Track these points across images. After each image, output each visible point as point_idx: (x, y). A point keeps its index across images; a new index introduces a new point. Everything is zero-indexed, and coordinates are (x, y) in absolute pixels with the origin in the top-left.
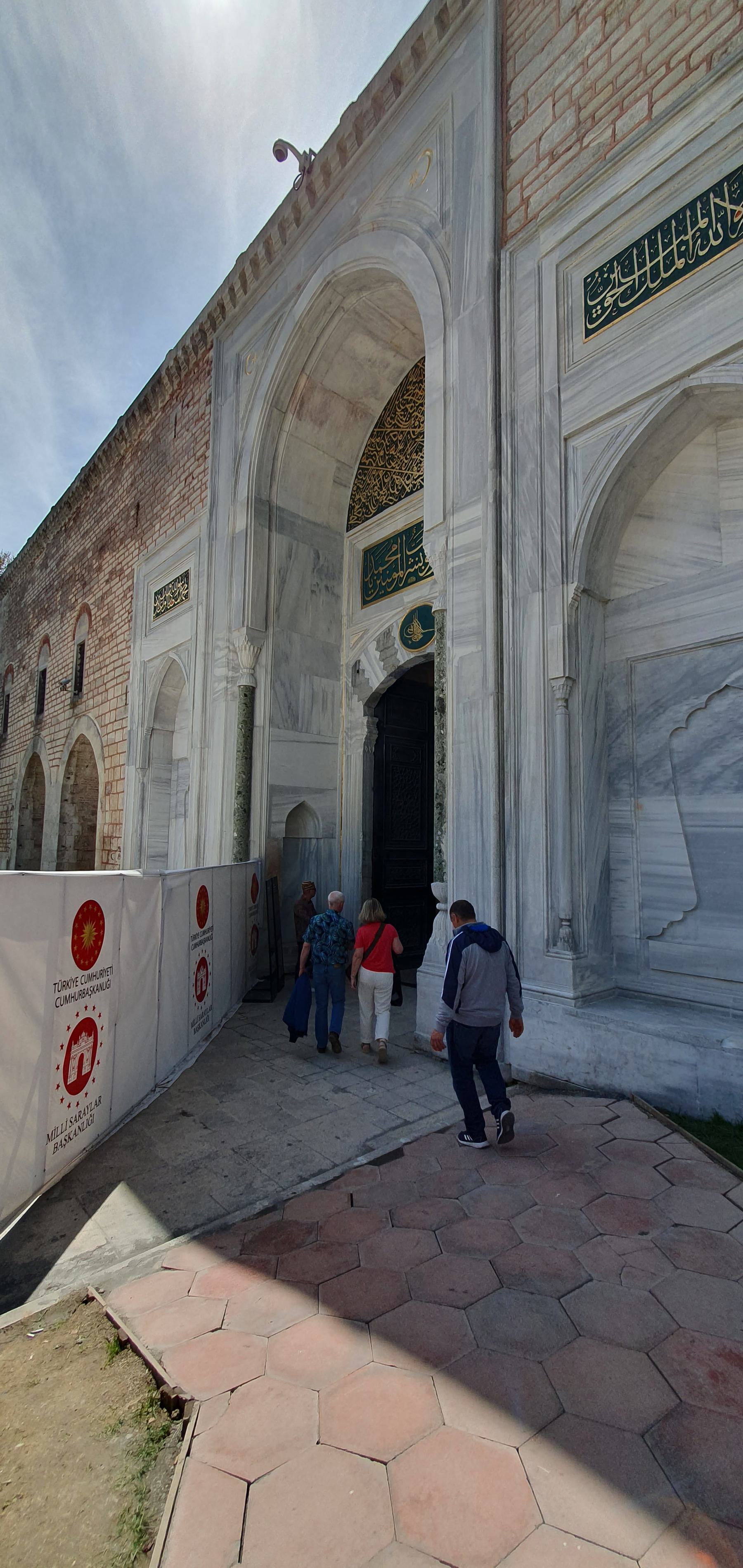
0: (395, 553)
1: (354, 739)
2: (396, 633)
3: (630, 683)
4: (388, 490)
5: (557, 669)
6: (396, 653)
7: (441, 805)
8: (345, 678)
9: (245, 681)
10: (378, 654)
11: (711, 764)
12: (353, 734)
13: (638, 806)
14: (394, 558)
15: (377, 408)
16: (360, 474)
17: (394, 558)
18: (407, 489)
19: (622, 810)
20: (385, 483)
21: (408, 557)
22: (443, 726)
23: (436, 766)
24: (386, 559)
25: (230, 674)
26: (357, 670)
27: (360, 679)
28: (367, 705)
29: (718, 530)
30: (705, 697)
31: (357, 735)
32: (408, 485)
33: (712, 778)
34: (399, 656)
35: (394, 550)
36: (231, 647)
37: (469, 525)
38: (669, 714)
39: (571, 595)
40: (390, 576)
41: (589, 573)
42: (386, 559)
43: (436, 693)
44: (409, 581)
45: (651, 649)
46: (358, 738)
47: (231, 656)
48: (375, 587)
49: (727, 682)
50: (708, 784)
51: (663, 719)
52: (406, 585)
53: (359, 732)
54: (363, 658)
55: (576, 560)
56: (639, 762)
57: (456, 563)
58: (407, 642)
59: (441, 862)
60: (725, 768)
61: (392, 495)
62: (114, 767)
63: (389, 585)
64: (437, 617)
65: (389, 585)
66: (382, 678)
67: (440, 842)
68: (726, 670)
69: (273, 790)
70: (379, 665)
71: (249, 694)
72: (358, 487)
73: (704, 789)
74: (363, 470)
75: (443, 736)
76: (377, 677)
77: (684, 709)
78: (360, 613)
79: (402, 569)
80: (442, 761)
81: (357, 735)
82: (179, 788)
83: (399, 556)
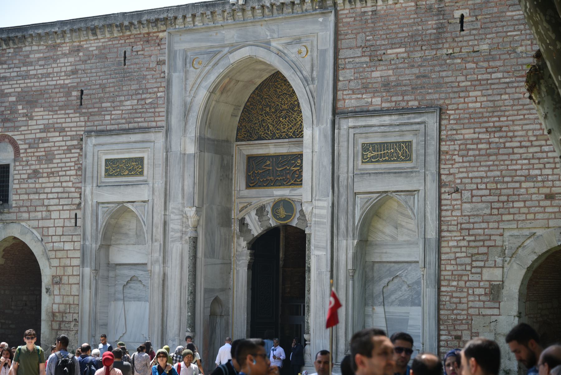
1: (241, 262)
2: (269, 209)
3: (373, 269)
4: (265, 130)
5: (350, 267)
6: (269, 219)
7: (308, 306)
8: (236, 227)
9: (193, 235)
10: (257, 217)
11: (393, 297)
13: (373, 309)
19: (369, 309)
20: (263, 126)
22: (309, 277)
23: (306, 292)
24: (263, 167)
25: (184, 229)
26: (242, 223)
27: (245, 229)
28: (248, 244)
29: (397, 228)
30: (392, 278)
31: (243, 259)
33: (393, 302)
34: (271, 222)
36: (185, 215)
37: (322, 208)
38: (383, 281)
39: (355, 243)
41: (361, 234)
43: (306, 265)
45: (378, 260)
47: (185, 220)
49: (398, 274)
50: (392, 303)
51: (381, 282)
53: (244, 258)
54: (247, 218)
55: (357, 233)
56: (374, 295)
57: (316, 220)
58: (275, 215)
59: (308, 327)
60: (396, 299)
61: (267, 134)
62: (64, 267)
64: (307, 236)
66: (260, 232)
67: (308, 320)
68: (397, 270)
69: (207, 291)
70: (258, 224)
71: (195, 240)
72: (244, 119)
73: (391, 305)
74: (246, 110)
75: (309, 281)
76: (256, 229)
77: (386, 280)
78: (246, 192)
80: (309, 291)
81: (243, 259)
82: (117, 282)
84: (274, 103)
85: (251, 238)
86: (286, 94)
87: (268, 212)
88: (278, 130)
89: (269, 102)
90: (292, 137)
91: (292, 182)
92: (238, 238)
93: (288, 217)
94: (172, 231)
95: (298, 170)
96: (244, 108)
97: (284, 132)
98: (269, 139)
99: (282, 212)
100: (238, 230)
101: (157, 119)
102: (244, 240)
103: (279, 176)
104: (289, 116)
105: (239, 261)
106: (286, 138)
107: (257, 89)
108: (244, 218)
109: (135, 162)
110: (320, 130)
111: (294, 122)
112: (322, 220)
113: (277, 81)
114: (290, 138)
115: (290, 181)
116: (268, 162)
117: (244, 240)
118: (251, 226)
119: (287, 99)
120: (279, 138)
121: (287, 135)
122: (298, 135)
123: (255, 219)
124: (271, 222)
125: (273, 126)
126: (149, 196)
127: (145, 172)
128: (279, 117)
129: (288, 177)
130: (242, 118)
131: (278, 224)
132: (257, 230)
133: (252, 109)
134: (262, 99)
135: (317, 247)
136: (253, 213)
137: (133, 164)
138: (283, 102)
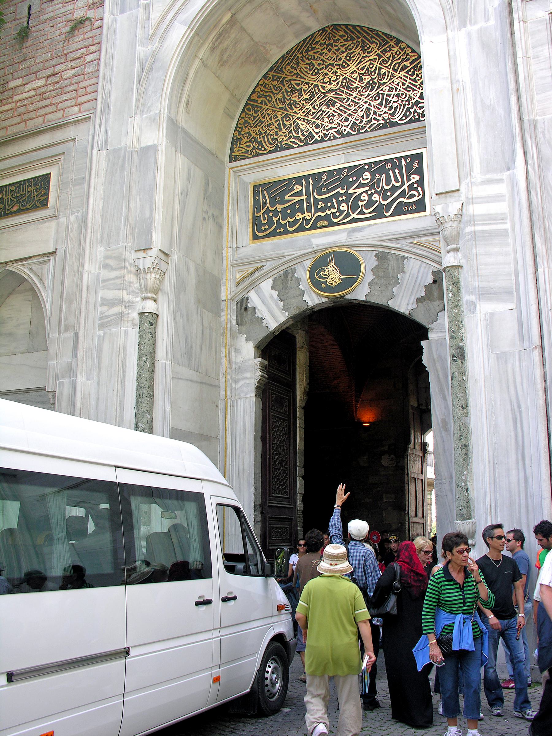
0: (300, 193)
10: (275, 294)
12: (240, 377)
14: (297, 199)
15: (276, 55)
16: (249, 110)
17: (297, 199)
18: (316, 137)
20: (285, 126)
21: (316, 201)
24: (287, 198)
27: (247, 317)
32: (317, 133)
34: (306, 298)
35: (296, 191)
40: (292, 215)
42: (287, 198)
44: (319, 224)
46: (247, 381)
48: (270, 222)
52: (314, 227)
63: (291, 224)
65: (291, 224)
76: (273, 315)
79: (309, 210)
83: (304, 197)
84: (308, 84)
85: (261, 335)
86: (332, 65)
87: (299, 280)
88: (317, 127)
89: (298, 85)
90: (349, 134)
91: (354, 216)
92: (234, 337)
93: (347, 284)
94: (102, 305)
95: (366, 192)
96: (247, 104)
97: (332, 128)
98: (299, 146)
99: (334, 275)
100: (234, 322)
101: (80, 100)
102: (247, 340)
103: (322, 210)
104: (341, 100)
105: (237, 382)
106: (335, 138)
107: (271, 70)
108: (247, 298)
109: (35, 185)
110: (469, 35)
111: (353, 108)
112: (494, 227)
113: (313, 49)
114: (343, 136)
115: (348, 215)
116: (298, 188)
117: (247, 340)
118: (262, 311)
119: (335, 73)
120: (322, 140)
121: (338, 132)
122: (363, 128)
123: (271, 296)
124: (306, 298)
125: (308, 122)
126: (56, 242)
127: (51, 201)
128: (320, 105)
129: (344, 207)
130: (242, 121)
131: (324, 300)
132: (274, 317)
133: (261, 103)
134: (282, 83)
135: (487, 294)
136: (266, 285)
137: (30, 189)
138: (327, 80)
